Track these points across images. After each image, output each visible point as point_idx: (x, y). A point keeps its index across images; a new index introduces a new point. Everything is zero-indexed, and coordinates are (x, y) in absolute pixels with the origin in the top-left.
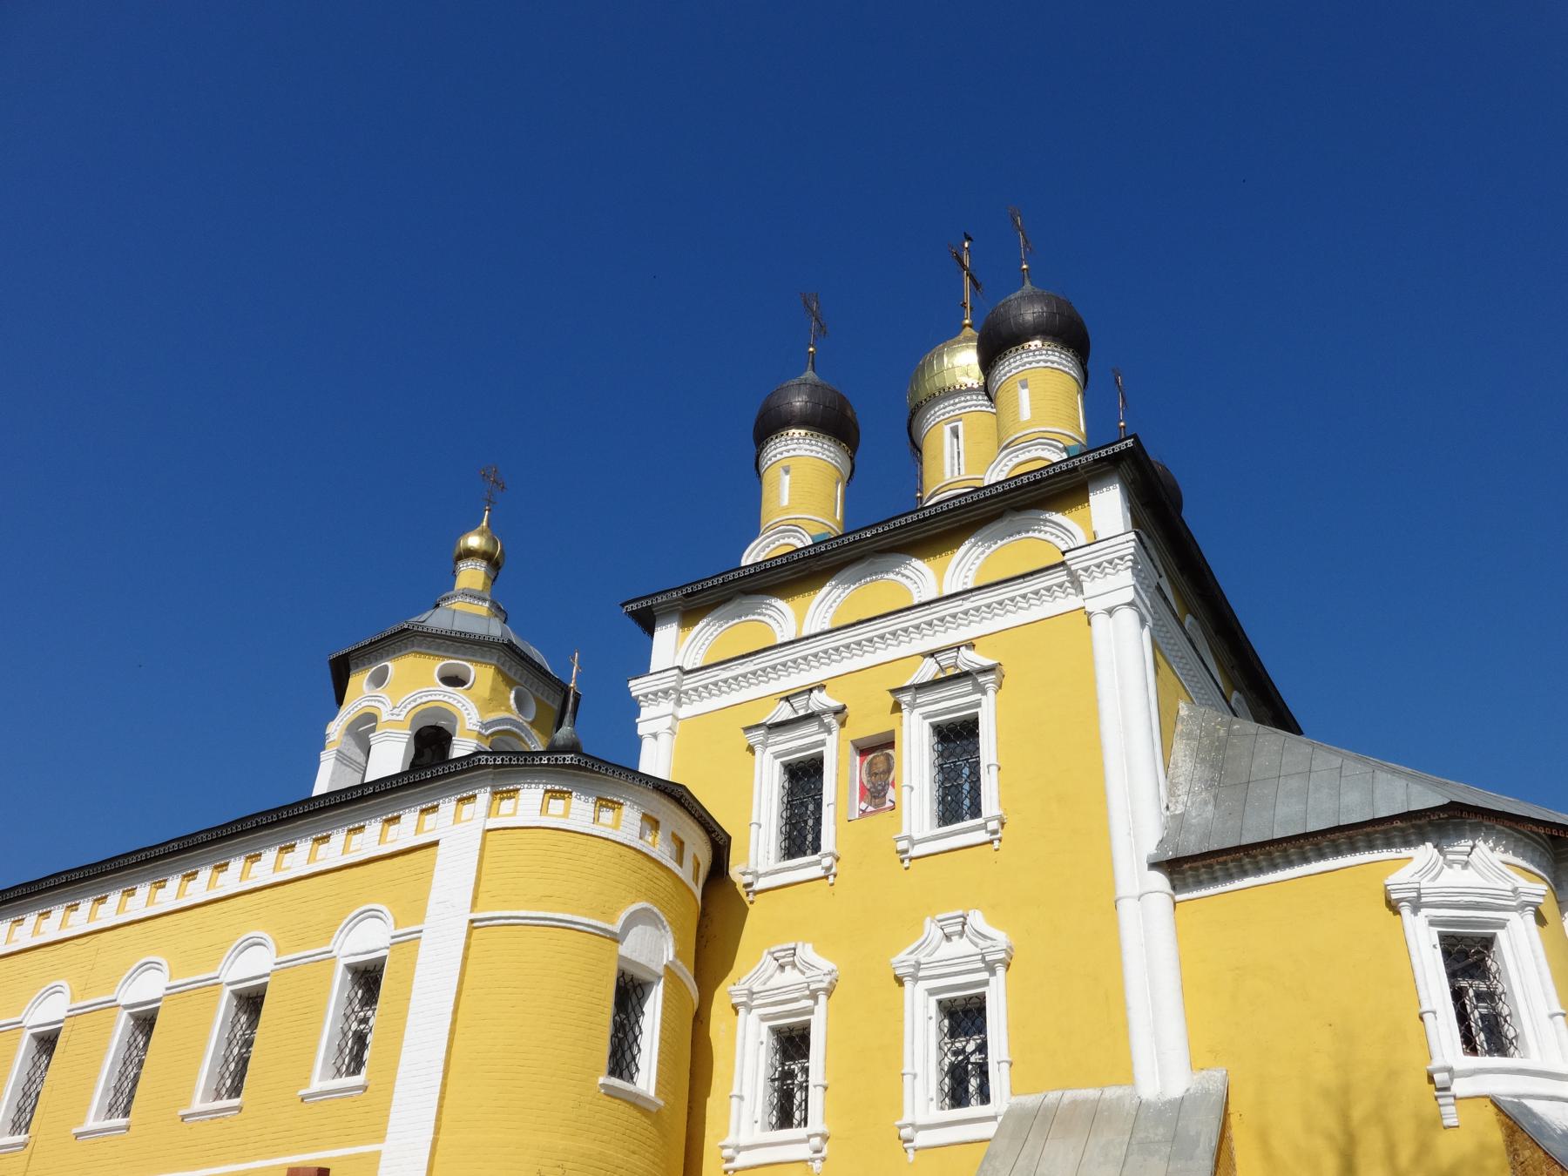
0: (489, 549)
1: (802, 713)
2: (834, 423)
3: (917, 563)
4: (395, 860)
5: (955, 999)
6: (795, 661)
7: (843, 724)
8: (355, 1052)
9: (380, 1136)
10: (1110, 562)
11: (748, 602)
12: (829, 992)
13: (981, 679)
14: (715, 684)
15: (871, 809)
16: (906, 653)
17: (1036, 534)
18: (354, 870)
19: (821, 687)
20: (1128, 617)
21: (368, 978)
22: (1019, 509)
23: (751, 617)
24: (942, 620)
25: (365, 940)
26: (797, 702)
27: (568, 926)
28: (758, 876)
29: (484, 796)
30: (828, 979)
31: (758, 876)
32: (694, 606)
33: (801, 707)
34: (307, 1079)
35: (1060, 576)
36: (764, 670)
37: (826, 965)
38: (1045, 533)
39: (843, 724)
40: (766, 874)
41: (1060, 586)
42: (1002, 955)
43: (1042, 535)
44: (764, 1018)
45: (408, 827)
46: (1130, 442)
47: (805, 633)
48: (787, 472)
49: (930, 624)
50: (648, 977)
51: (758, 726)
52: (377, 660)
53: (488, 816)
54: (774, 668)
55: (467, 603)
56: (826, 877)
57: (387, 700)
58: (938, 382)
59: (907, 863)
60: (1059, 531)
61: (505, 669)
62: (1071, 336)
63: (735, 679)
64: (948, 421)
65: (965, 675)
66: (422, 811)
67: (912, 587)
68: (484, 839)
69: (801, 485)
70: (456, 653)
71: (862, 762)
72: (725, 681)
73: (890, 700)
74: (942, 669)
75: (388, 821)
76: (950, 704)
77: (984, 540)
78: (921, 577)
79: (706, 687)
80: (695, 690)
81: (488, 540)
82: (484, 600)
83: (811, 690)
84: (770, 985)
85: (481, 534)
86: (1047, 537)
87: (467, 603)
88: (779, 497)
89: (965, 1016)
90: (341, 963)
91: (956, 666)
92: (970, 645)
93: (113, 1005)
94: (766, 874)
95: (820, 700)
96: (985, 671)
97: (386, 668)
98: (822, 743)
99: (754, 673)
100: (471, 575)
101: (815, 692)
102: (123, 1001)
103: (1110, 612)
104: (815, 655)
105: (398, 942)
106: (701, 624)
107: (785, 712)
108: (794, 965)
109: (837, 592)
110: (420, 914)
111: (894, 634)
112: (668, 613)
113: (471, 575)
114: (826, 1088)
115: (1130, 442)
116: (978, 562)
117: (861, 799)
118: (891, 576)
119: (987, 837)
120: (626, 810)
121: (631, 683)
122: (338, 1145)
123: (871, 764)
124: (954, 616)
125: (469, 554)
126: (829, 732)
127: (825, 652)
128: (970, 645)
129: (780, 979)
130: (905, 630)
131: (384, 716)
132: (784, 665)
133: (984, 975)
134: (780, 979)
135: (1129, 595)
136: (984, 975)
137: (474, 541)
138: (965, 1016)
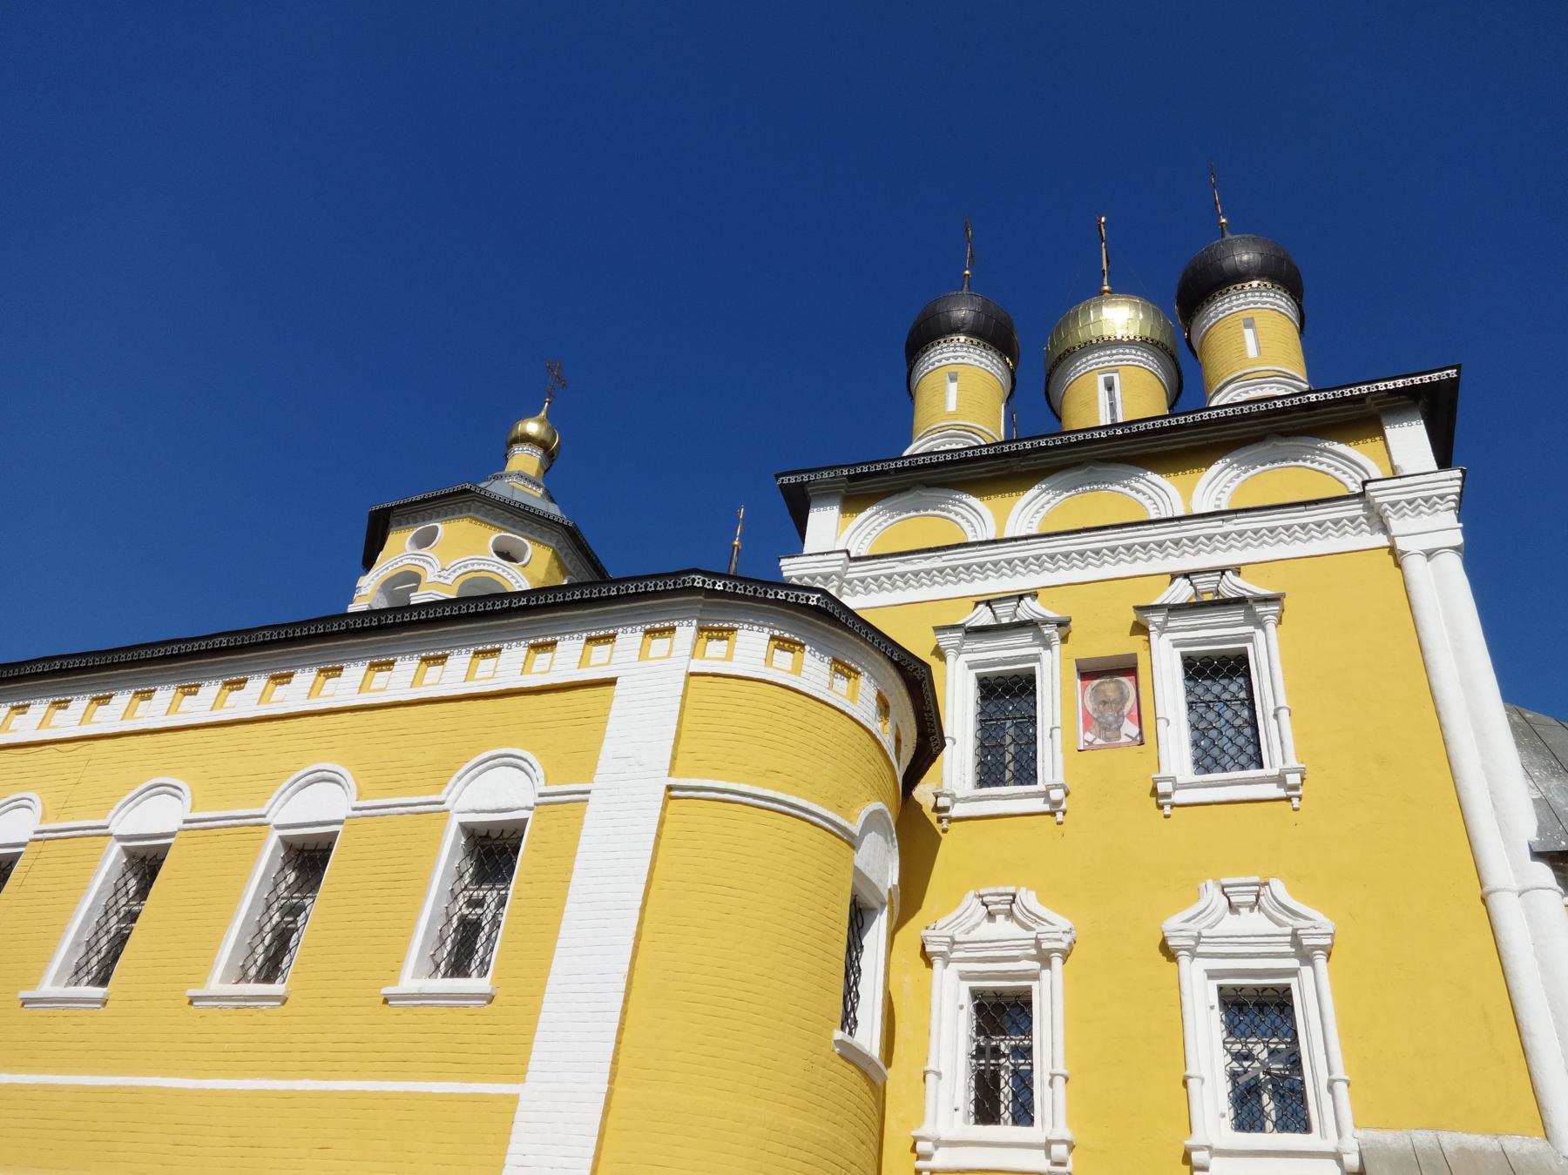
0: (549, 439)
1: (1005, 620)
3: (1151, 476)
4: (544, 697)
5: (1242, 988)
6: (995, 564)
7: (1064, 639)
8: (464, 947)
9: (516, 1069)
10: (1426, 500)
11: (929, 494)
12: (1066, 955)
13: (1260, 609)
14: (889, 577)
15: (1099, 741)
17: (1308, 464)
18: (481, 703)
19: (1034, 595)
20: (1453, 566)
21: (493, 852)
22: (1287, 434)
23: (930, 512)
24: (1193, 540)
25: (493, 795)
27: (801, 815)
28: (955, 800)
29: (686, 632)
30: (1068, 938)
31: (955, 800)
32: (858, 493)
33: (1005, 614)
34: (394, 973)
35: (1356, 509)
36: (954, 569)
37: (1063, 923)
38: (1324, 463)
39: (1064, 639)
40: (966, 800)
41: (1352, 520)
42: (1327, 941)
43: (1315, 466)
44: (964, 976)
45: (570, 657)
46: (1452, 373)
47: (1007, 535)
48: (953, 378)
49: (1177, 543)
50: (876, 904)
51: (954, 628)
52: (424, 520)
53: (693, 656)
54: (967, 568)
56: (1053, 814)
57: (436, 561)
58: (1093, 332)
59: (1167, 810)
60: (1343, 463)
61: (561, 555)
63: (916, 574)
64: (1101, 371)
65: (1240, 601)
66: (589, 640)
67: (1147, 503)
68: (686, 684)
69: (960, 395)
70: (514, 527)
71: (1084, 688)
72: (902, 575)
73: (1133, 617)
74: (1196, 593)
75: (536, 647)
76: (1214, 633)
77: (1240, 463)
79: (876, 579)
80: (862, 580)
81: (548, 429)
82: (539, 486)
83: (1021, 597)
84: (974, 936)
85: (541, 422)
86: (1323, 468)
88: (944, 401)
89: (1258, 1009)
90: (454, 822)
91: (1218, 593)
92: (1237, 571)
93: (102, 832)
94: (966, 800)
96: (1266, 600)
97: (436, 529)
98: (1036, 658)
99: (941, 571)
100: (525, 460)
101: (1028, 599)
102: (117, 829)
103: (1429, 554)
104: (1023, 561)
105: (546, 802)
106: (869, 511)
107: (984, 617)
108: (1010, 915)
109: (1045, 498)
110: (589, 771)
111: (1128, 548)
112: (826, 495)
113: (525, 460)
114: (1067, 1080)
115: (1452, 373)
116: (1233, 486)
117: (1086, 729)
118: (1117, 488)
119: (1281, 793)
120: (863, 681)
121: (783, 562)
122: (438, 1076)
123: (1096, 690)
124: (1210, 538)
125: (527, 439)
126: (1047, 645)
127: (1037, 558)
128: (1237, 571)
129: (987, 930)
130: (1144, 546)
132: (981, 566)
133: (1293, 963)
134: (987, 930)
135: (1458, 539)
136: (1293, 963)
137: (532, 427)
138: (1258, 1009)
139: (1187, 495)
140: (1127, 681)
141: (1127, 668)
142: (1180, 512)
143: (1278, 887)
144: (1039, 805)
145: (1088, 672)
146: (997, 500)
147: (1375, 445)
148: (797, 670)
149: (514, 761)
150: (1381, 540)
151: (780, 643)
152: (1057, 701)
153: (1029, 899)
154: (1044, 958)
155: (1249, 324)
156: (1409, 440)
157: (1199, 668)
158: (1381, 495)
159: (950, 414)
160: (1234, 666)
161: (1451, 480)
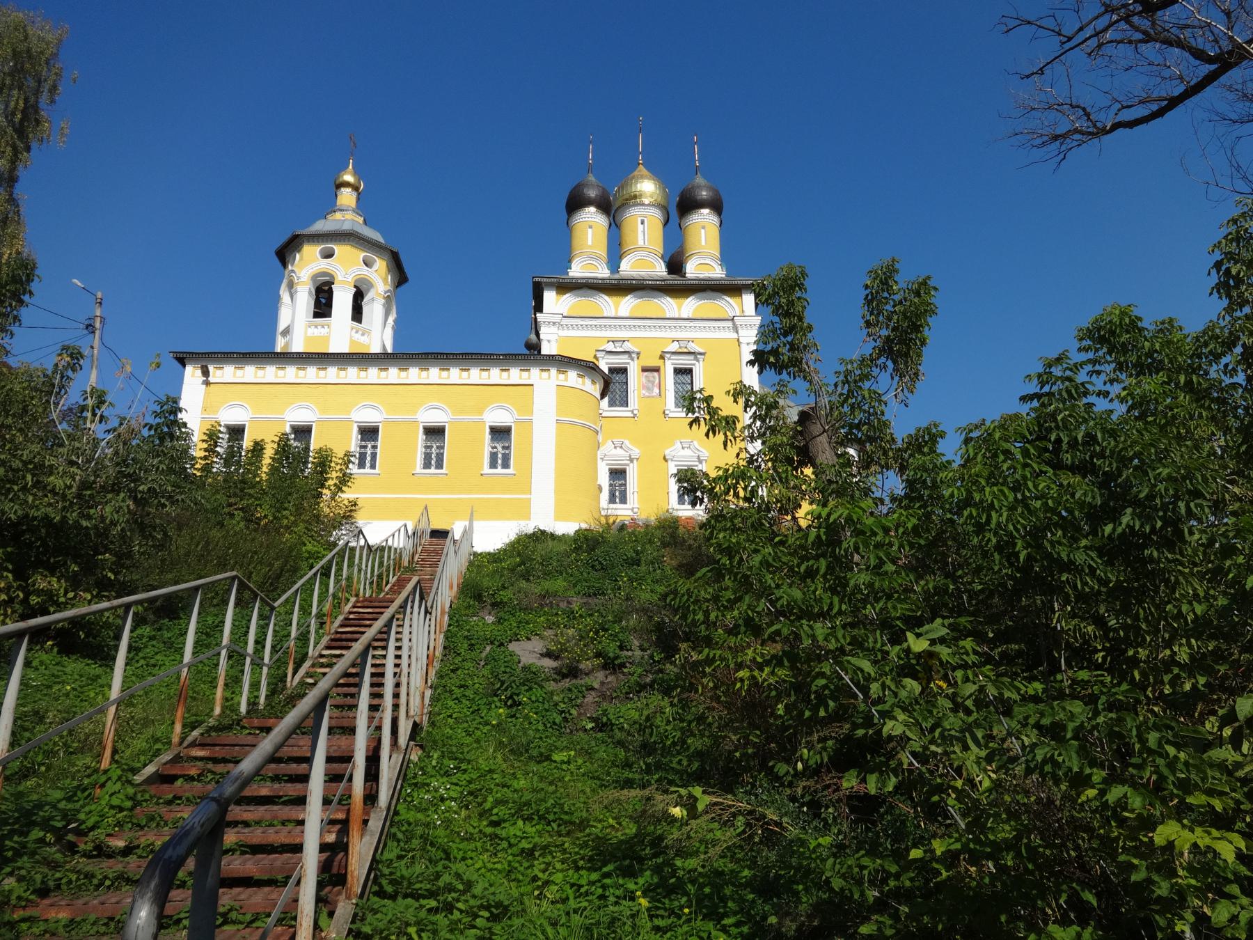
2: (605, 206)
16: (666, 336)
25: (500, 418)
26: (617, 344)
27: (588, 427)
35: (730, 324)
37: (637, 451)
55: (346, 210)
60: (728, 305)
62: (716, 206)
76: (684, 362)
78: (669, 306)
87: (346, 210)
95: (627, 346)
100: (347, 197)
107: (611, 347)
113: (347, 197)
125: (347, 184)
129: (614, 452)
131: (339, 277)
134: (614, 452)
137: (348, 178)
139: (680, 308)
140: (656, 374)
141: (657, 370)
142: (677, 316)
143: (696, 443)
144: (630, 414)
145: (645, 370)
146: (615, 298)
147: (738, 300)
148: (584, 384)
149: (505, 408)
150: (735, 336)
151: (580, 376)
152: (635, 378)
153: (627, 443)
154: (632, 460)
155: (703, 228)
156: (749, 299)
157: (678, 371)
158: (738, 321)
159: (590, 247)
160: (689, 372)
161: (757, 320)
